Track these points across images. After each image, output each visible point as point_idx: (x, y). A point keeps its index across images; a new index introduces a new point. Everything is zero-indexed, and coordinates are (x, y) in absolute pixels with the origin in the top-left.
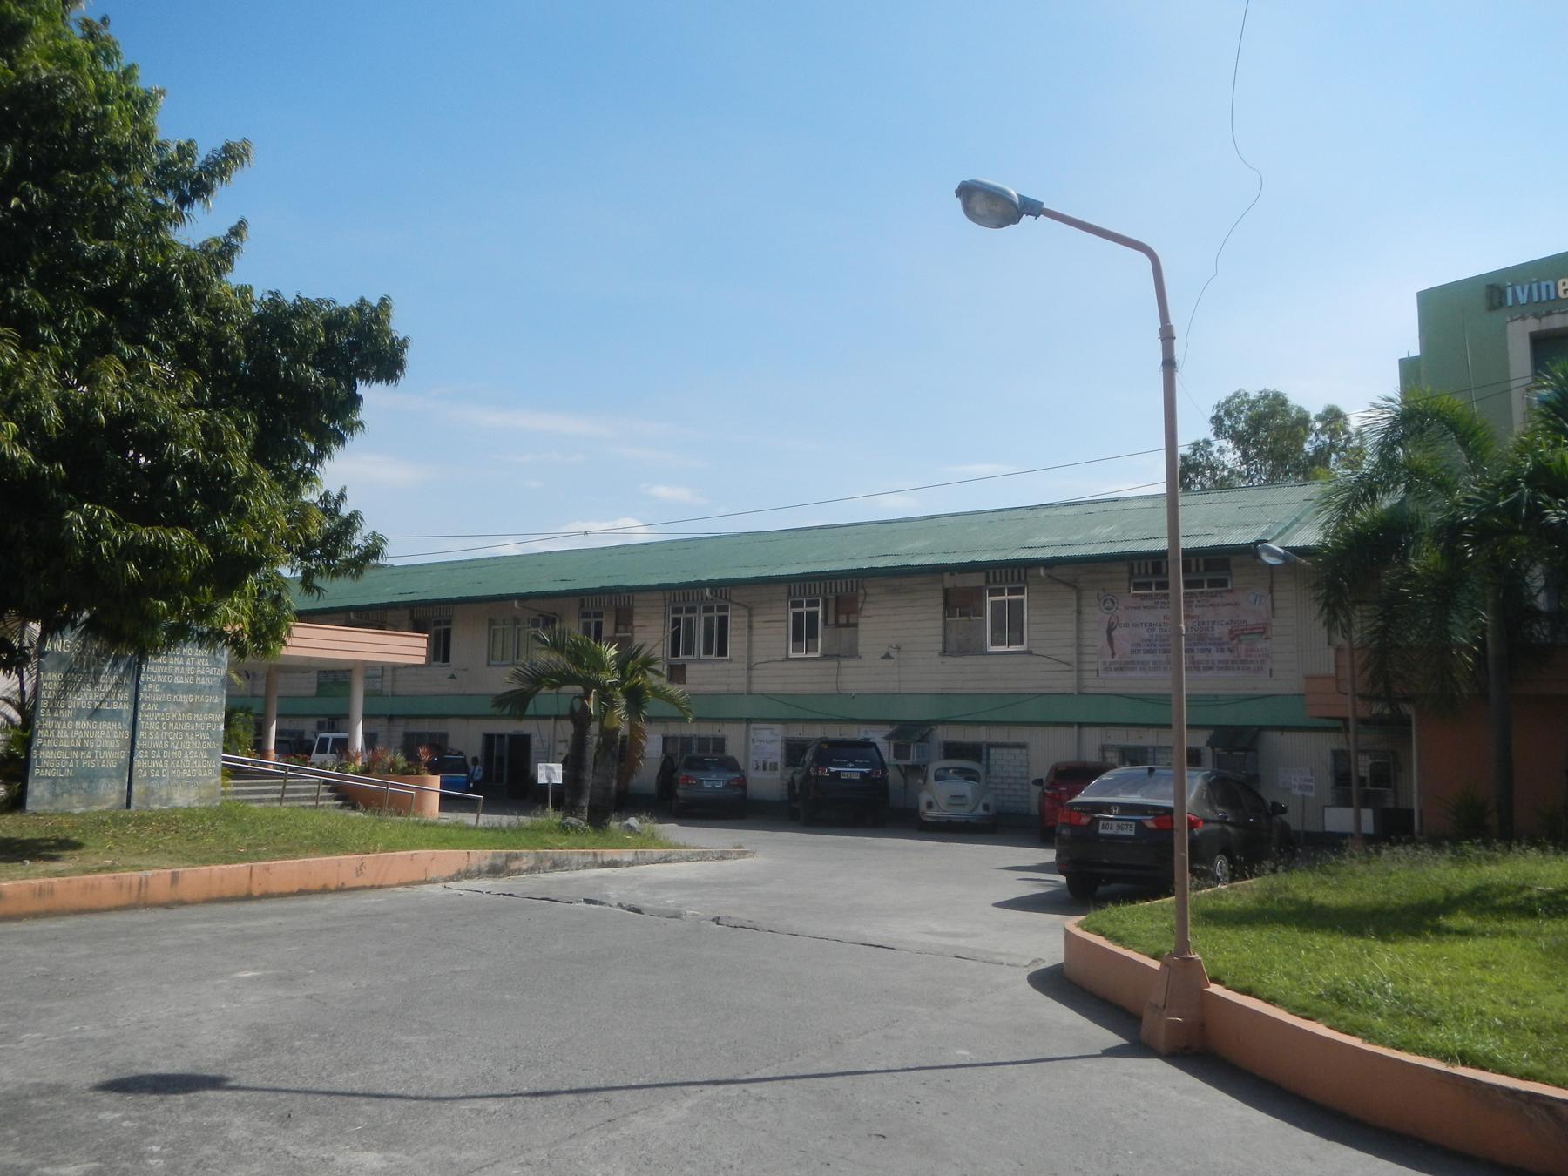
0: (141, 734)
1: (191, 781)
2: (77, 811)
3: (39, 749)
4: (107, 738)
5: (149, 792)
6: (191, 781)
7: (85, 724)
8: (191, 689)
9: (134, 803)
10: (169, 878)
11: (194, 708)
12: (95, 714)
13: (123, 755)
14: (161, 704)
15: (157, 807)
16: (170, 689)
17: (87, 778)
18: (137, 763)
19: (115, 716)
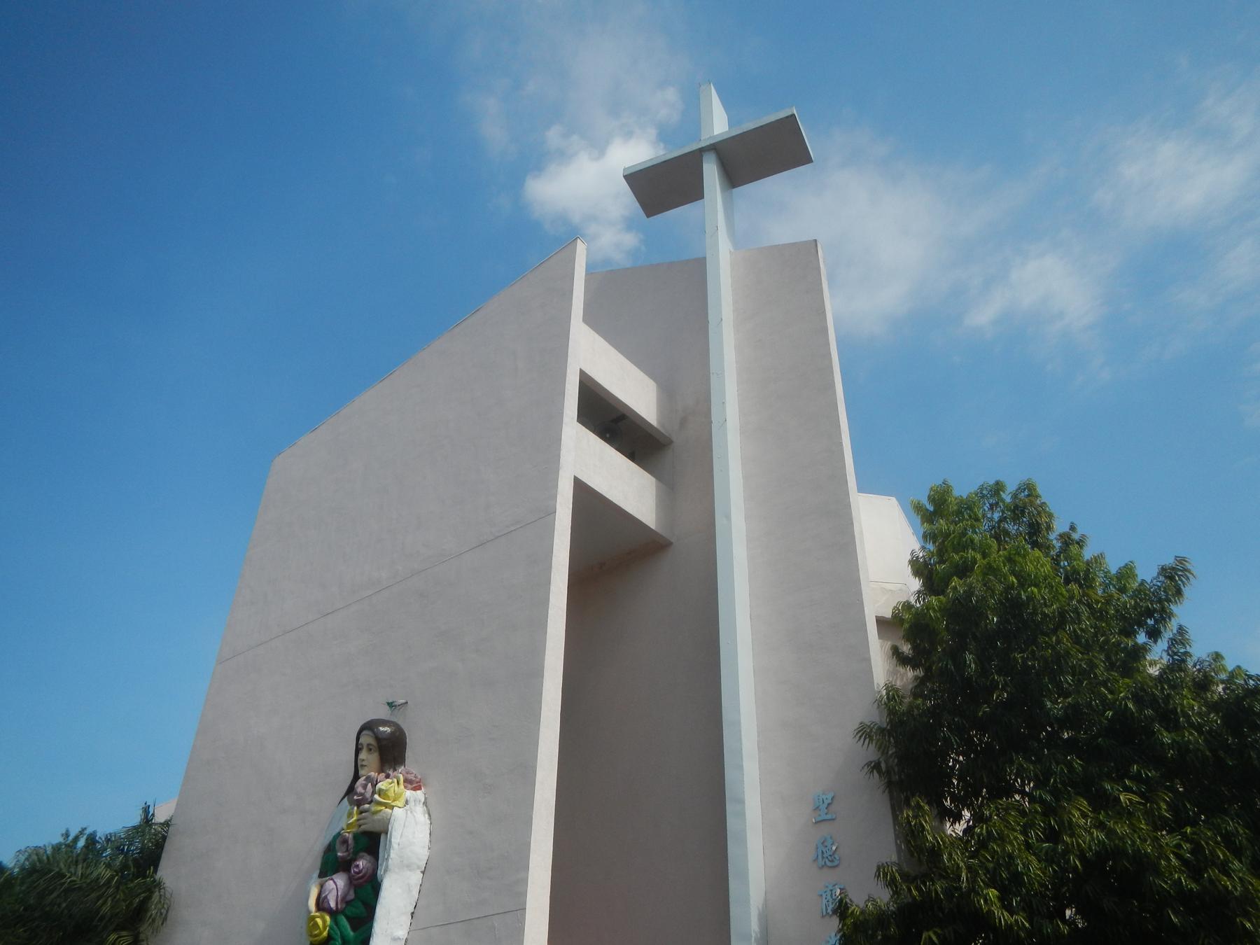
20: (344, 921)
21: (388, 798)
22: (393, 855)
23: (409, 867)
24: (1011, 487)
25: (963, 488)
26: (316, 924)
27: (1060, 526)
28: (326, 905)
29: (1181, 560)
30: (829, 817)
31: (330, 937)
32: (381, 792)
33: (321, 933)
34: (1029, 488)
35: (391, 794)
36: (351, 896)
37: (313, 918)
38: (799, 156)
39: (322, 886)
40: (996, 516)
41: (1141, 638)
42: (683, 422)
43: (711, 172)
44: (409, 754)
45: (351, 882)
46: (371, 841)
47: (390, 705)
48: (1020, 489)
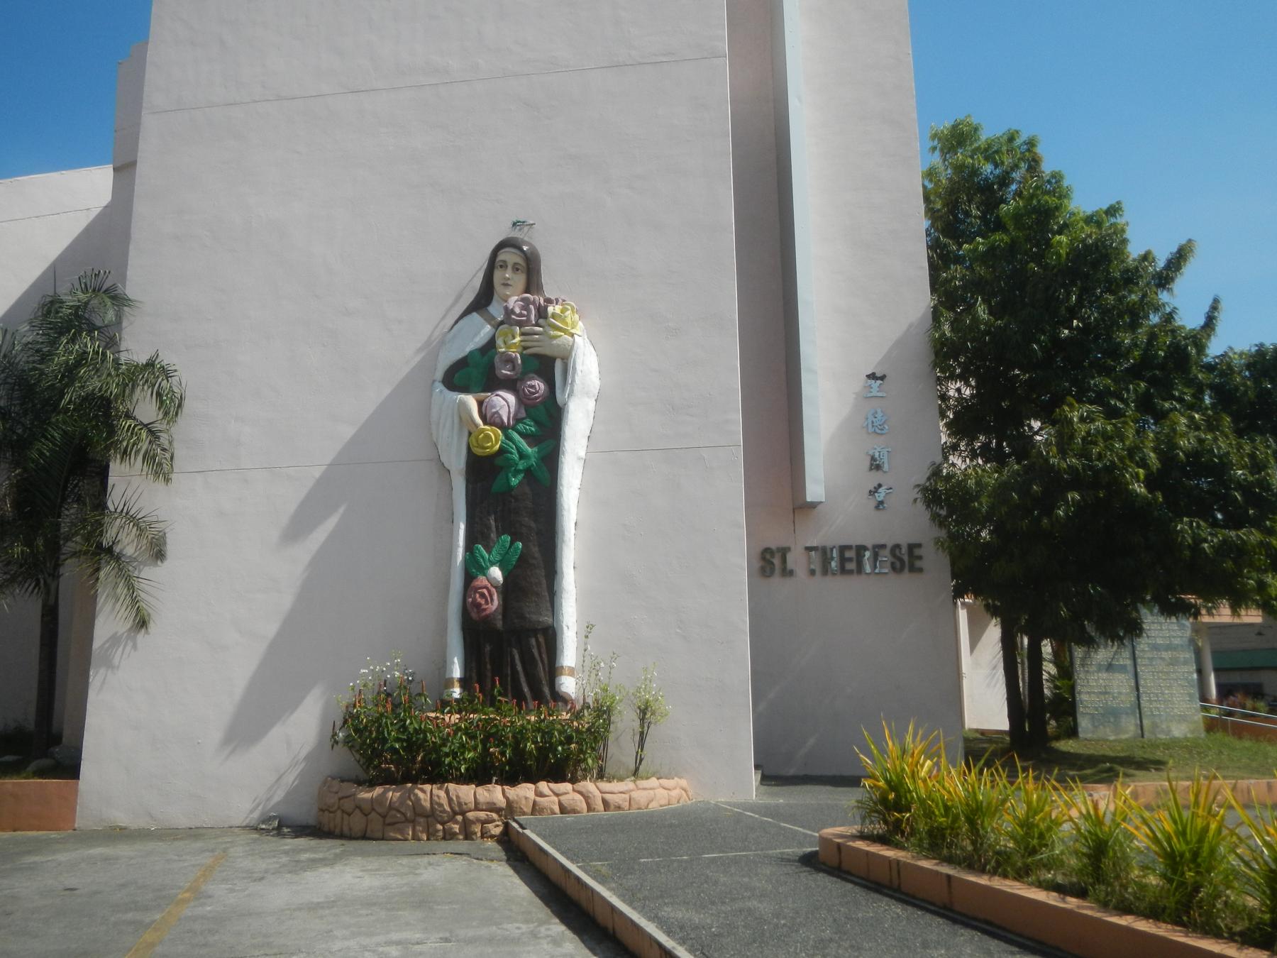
0: (1142, 682)
1: (1182, 719)
2: (1112, 738)
3: (1080, 693)
4: (1120, 684)
5: (1155, 725)
6: (1182, 719)
7: (1105, 675)
8: (1169, 648)
9: (1147, 734)
10: (1265, 789)
11: (1174, 662)
12: (1110, 667)
14: (1151, 659)
15: (1162, 736)
16: (1155, 647)
17: (1111, 715)
18: (1143, 704)
19: (1122, 669)
20: (516, 436)
21: (566, 324)
22: (577, 379)
23: (587, 394)
26: (488, 438)
28: (498, 420)
30: (880, 394)
31: (502, 451)
32: (554, 316)
33: (492, 446)
34: (1031, 144)
35: (568, 320)
36: (523, 414)
37: (483, 431)
39: (480, 403)
44: (545, 279)
45: (520, 400)
46: (548, 366)
47: (514, 224)
48: (1025, 143)
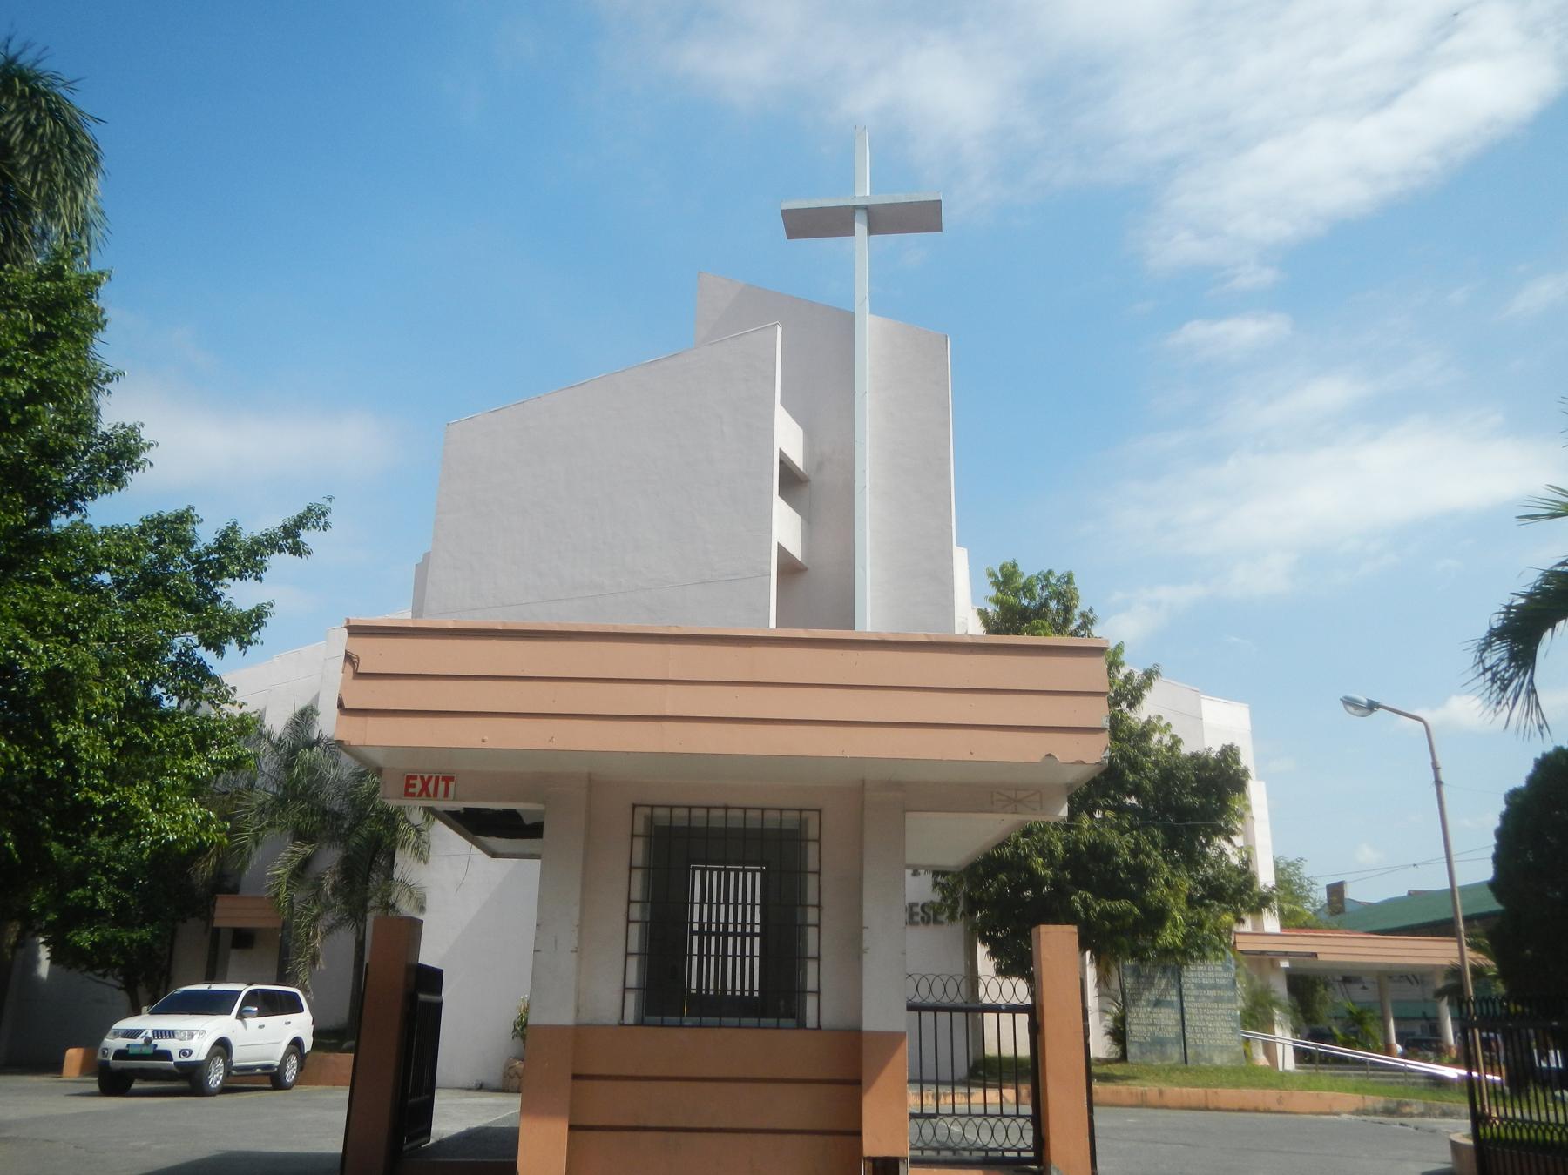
12: (1157, 1003)
13: (1178, 1029)
19: (1170, 1004)
24: (1058, 574)
25: (1029, 570)
27: (1081, 607)
29: (1156, 665)
34: (1069, 579)
38: (936, 226)
40: (1045, 594)
41: (1124, 705)
42: (820, 467)
43: (861, 228)
